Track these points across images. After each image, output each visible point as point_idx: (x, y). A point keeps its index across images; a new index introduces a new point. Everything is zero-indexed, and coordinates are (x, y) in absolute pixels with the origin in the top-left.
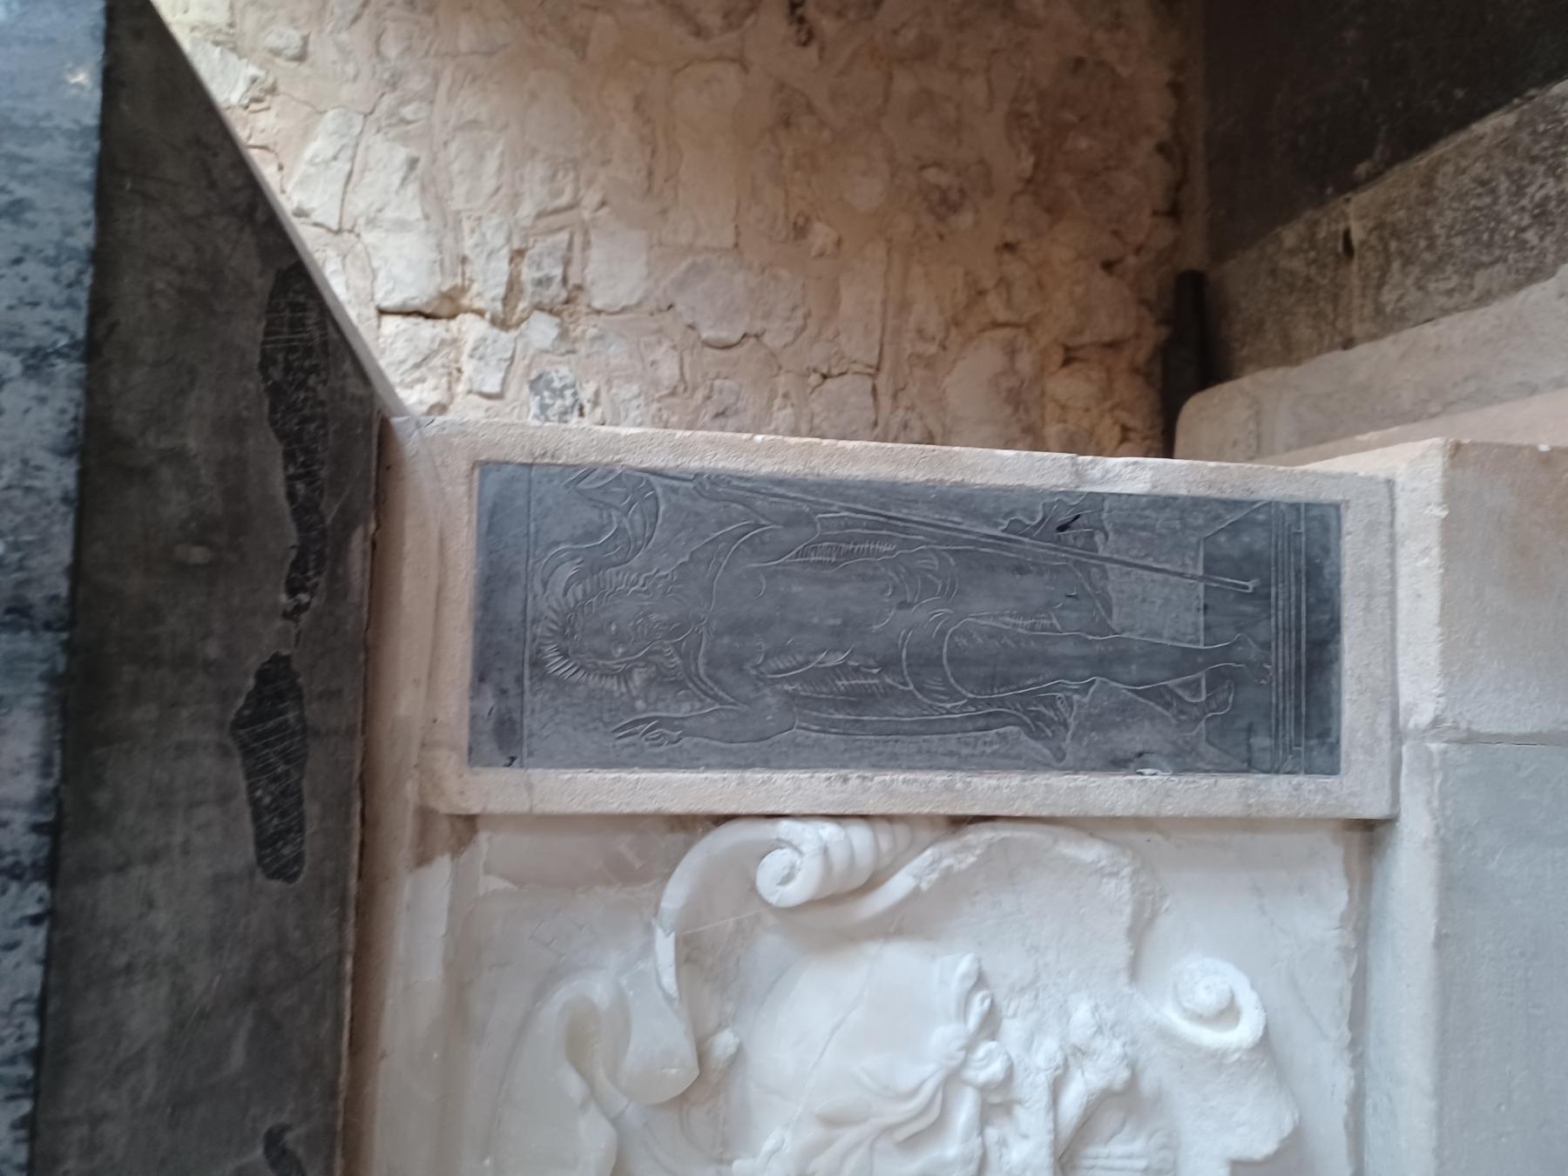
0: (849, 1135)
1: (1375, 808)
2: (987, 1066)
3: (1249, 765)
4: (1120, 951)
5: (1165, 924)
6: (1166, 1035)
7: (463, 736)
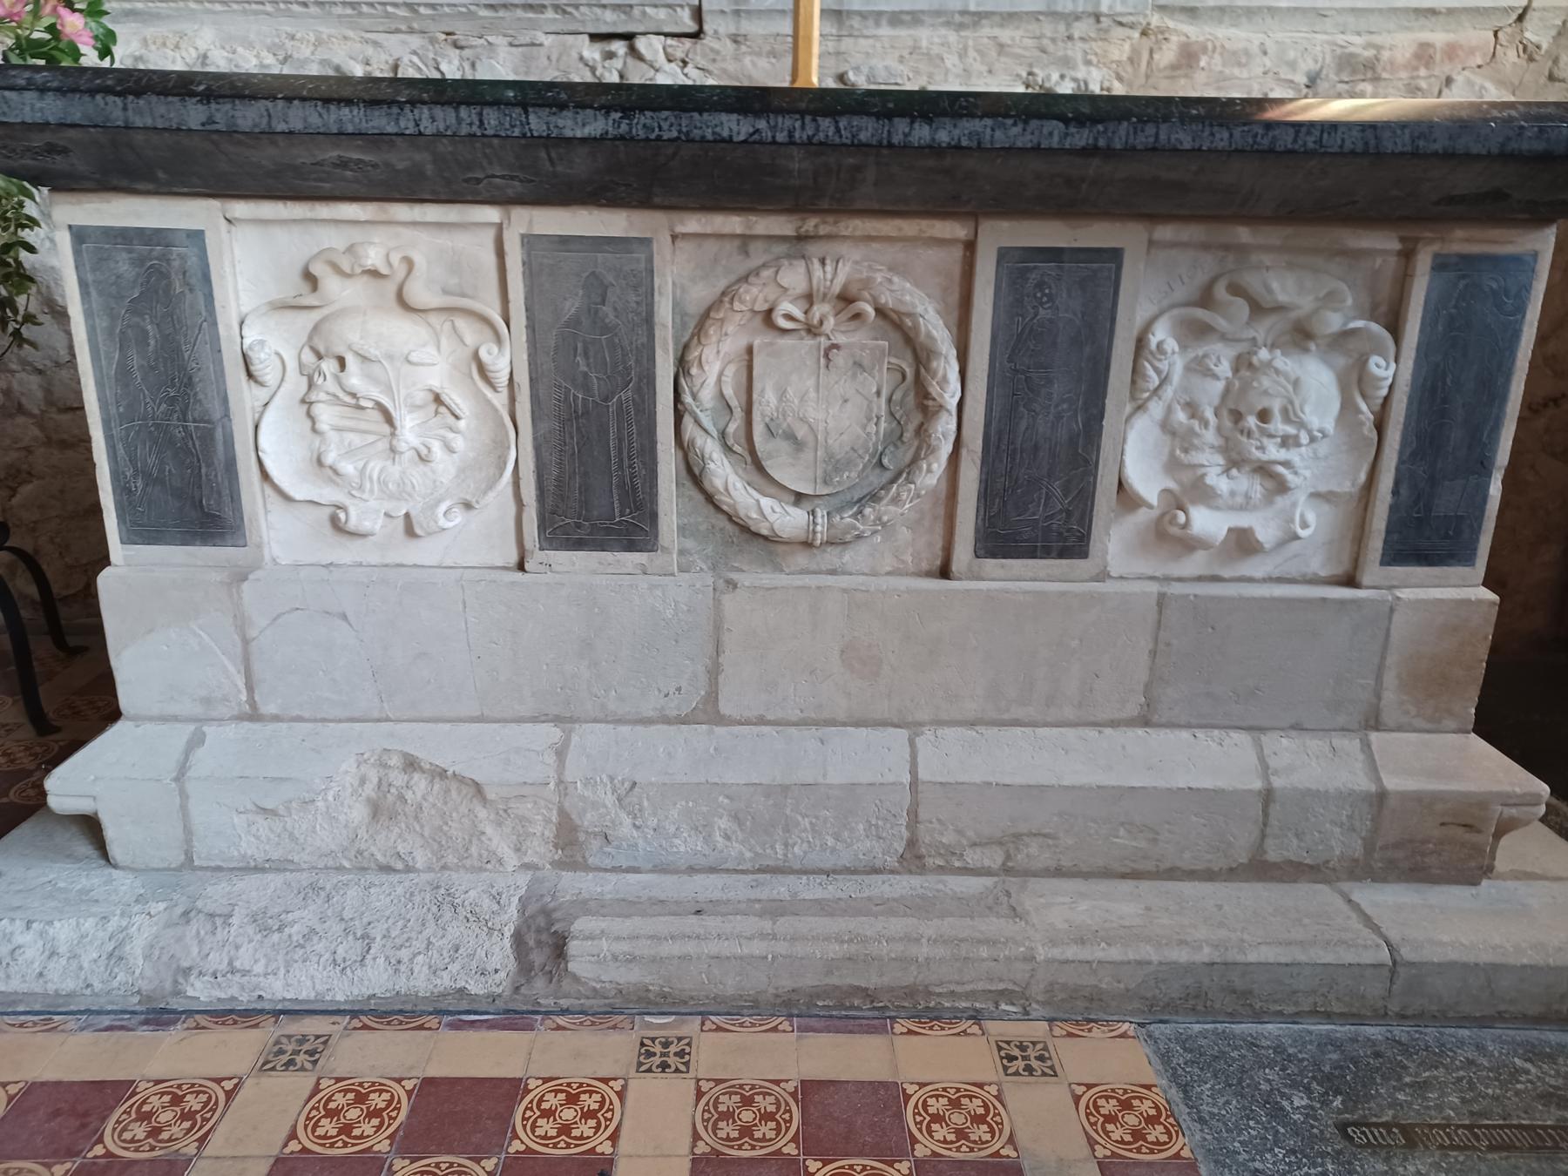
0: (1290, 388)
1: (1366, 579)
2: (1304, 438)
3: (1388, 531)
4: (1323, 488)
5: (1326, 507)
6: (1294, 505)
7: (1445, 251)
